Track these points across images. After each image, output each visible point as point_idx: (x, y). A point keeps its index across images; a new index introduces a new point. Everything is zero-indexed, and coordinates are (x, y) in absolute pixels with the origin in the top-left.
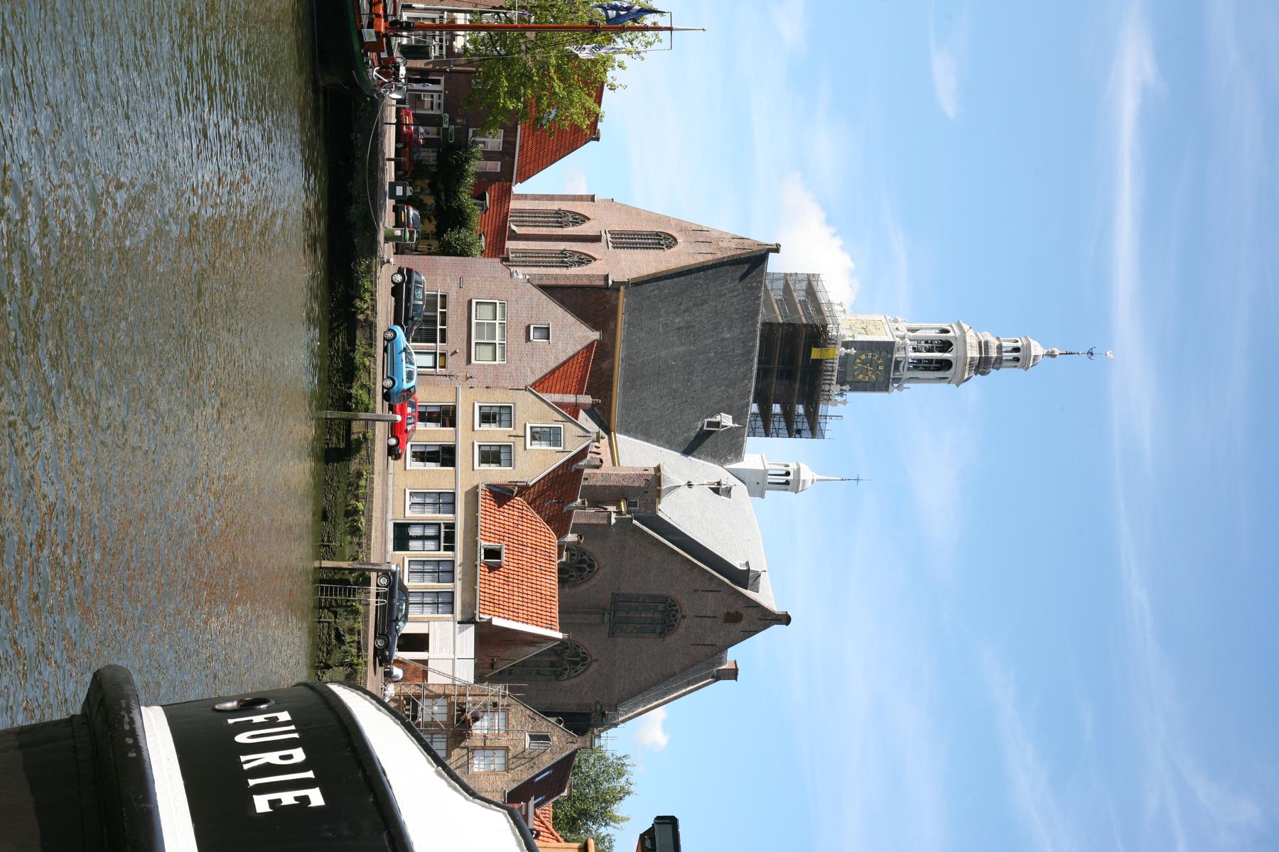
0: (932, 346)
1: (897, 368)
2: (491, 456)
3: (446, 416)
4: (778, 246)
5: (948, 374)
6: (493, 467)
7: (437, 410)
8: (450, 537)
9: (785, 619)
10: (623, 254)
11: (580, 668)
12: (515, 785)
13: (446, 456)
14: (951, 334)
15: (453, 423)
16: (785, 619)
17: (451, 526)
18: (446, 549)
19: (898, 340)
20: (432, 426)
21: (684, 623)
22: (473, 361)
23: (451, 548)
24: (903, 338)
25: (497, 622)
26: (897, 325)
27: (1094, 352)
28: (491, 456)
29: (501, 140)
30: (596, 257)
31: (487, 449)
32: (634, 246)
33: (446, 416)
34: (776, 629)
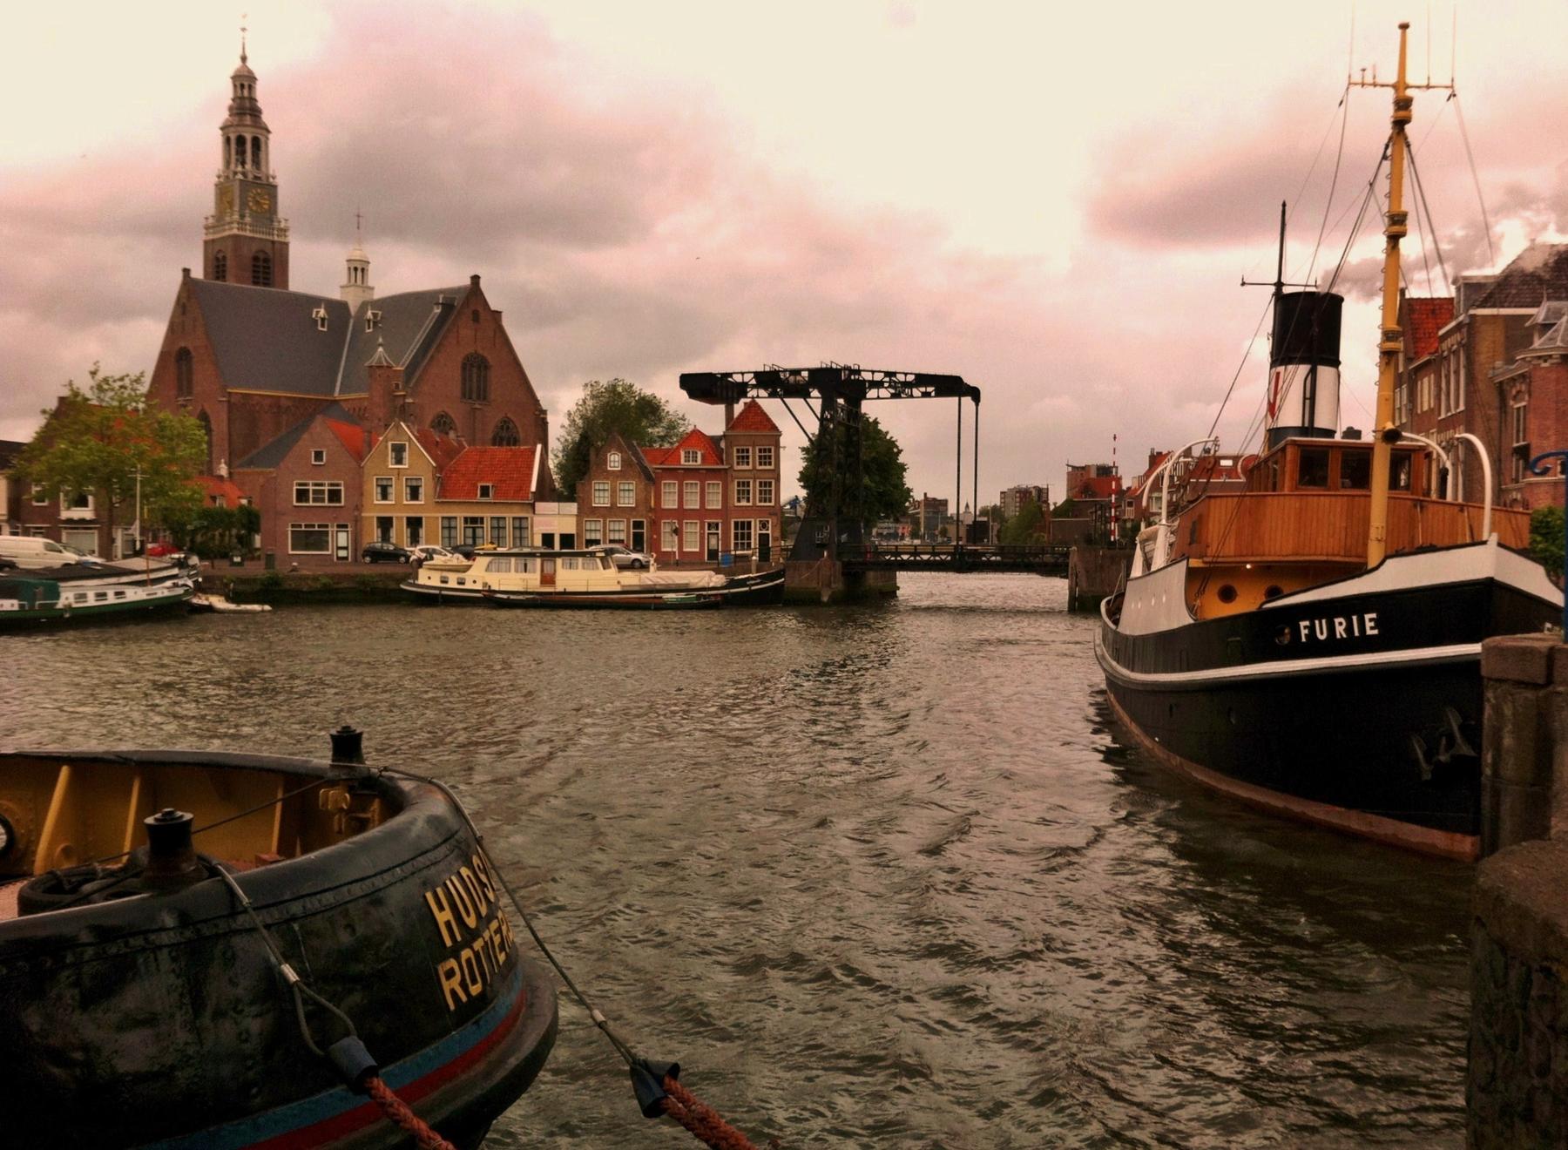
0: (241, 152)
1: (259, 178)
2: (414, 493)
3: (385, 524)
5: (262, 139)
6: (422, 491)
8: (474, 520)
9: (475, 279)
11: (511, 425)
13: (415, 524)
15: (390, 519)
16: (475, 279)
17: (466, 519)
18: (482, 523)
20: (393, 532)
21: (481, 352)
23: (482, 519)
25: (533, 488)
28: (414, 493)
32: (190, 381)
33: (385, 524)
34: (483, 285)
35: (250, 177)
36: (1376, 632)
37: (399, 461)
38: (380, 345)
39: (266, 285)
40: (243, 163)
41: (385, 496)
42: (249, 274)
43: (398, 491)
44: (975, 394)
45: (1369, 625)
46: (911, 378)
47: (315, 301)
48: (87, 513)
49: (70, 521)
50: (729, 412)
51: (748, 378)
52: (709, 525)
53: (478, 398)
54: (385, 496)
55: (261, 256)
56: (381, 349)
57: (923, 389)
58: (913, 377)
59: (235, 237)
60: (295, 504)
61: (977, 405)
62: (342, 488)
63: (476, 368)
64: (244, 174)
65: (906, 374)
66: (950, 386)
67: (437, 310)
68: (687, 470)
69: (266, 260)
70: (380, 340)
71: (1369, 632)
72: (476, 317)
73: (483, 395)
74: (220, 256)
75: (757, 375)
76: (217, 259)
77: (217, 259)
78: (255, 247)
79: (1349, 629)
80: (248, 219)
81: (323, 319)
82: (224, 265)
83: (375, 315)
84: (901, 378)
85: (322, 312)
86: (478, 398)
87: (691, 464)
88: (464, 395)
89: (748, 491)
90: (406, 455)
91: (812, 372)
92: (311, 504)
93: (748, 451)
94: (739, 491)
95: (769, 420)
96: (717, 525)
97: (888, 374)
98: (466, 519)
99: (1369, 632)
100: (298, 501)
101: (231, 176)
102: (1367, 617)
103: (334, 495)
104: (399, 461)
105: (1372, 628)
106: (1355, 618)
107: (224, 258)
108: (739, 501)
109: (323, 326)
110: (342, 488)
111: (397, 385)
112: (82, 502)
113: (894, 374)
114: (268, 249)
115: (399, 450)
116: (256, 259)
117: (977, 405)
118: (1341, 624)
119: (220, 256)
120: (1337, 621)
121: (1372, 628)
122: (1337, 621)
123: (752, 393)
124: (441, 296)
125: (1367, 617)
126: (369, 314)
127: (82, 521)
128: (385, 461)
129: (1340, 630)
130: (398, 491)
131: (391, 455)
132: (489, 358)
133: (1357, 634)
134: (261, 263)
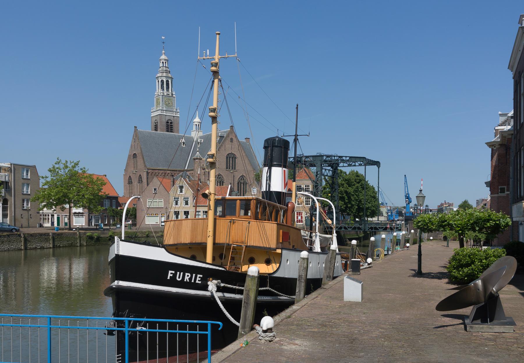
1: (169, 94)
2: (187, 203)
3: (177, 214)
6: (189, 202)
17: (203, 211)
22: (163, 207)
27: (163, 42)
28: (187, 203)
29: (107, 200)
31: (184, 203)
33: (177, 214)
35: (165, 94)
36: (200, 282)
37: (181, 192)
38: (198, 151)
39: (172, 132)
42: (165, 128)
43: (181, 202)
44: (377, 164)
45: (198, 279)
46: (348, 158)
49: (75, 213)
53: (232, 169)
54: (177, 204)
55: (170, 121)
57: (359, 163)
58: (349, 158)
65: (346, 157)
69: (171, 123)
70: (198, 150)
71: (197, 282)
72: (232, 140)
73: (234, 167)
76: (155, 123)
78: (167, 118)
79: (190, 279)
81: (184, 143)
82: (157, 125)
83: (201, 141)
86: (232, 169)
88: (227, 168)
90: (184, 189)
97: (340, 157)
98: (203, 211)
99: (197, 282)
102: (199, 276)
104: (181, 192)
105: (199, 280)
106: (194, 275)
107: (157, 122)
109: (183, 145)
113: (342, 157)
114: (172, 118)
115: (181, 187)
116: (167, 122)
118: (188, 276)
119: (156, 122)
120: (187, 274)
121: (199, 280)
122: (187, 274)
124: (220, 133)
125: (199, 276)
127: (79, 213)
129: (187, 278)
130: (181, 202)
131: (179, 190)
132: (236, 155)
133: (193, 281)
134: (169, 124)
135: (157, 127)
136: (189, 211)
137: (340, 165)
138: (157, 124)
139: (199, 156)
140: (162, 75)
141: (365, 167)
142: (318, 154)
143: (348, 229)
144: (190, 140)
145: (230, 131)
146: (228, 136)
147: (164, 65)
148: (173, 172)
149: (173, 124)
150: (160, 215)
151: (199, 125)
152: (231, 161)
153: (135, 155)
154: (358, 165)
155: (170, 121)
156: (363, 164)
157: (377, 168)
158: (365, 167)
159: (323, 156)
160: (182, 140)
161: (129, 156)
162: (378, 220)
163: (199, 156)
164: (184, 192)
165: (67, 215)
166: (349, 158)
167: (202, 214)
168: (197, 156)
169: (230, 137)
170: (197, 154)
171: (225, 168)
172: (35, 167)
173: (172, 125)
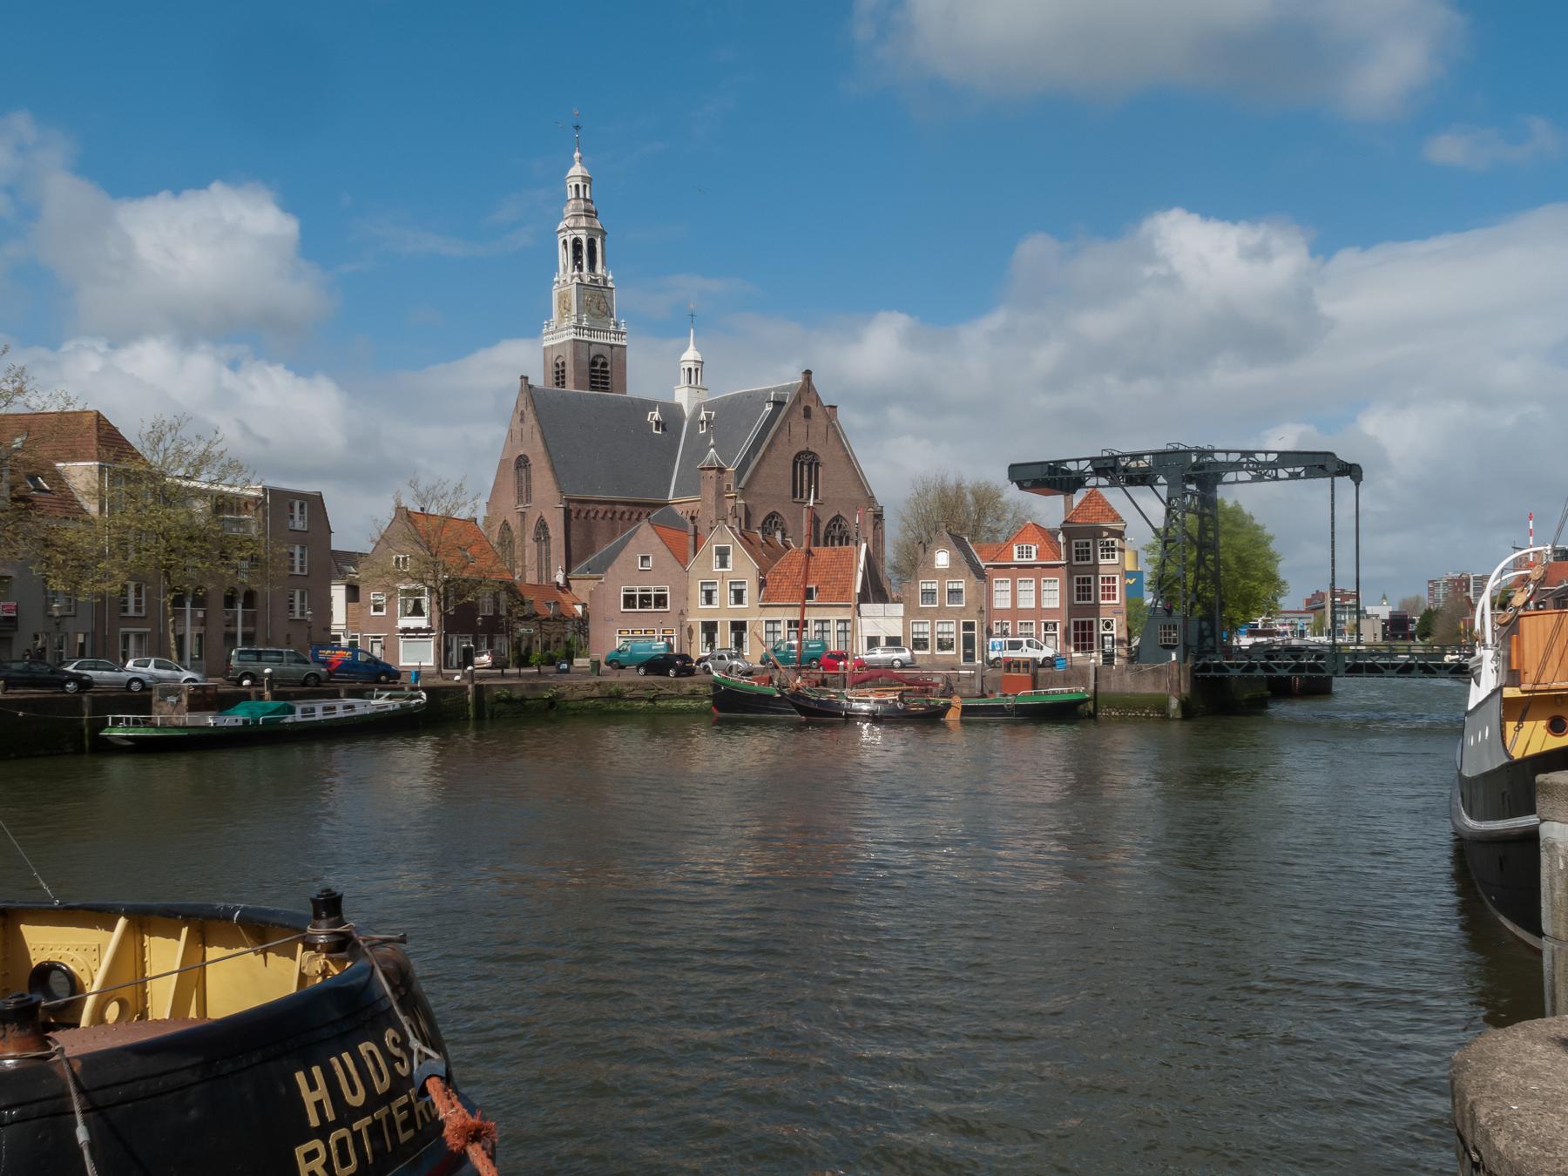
1: (596, 281)
2: (739, 597)
3: (710, 628)
4: (522, 377)
6: (745, 593)
7: (704, 635)
9: (808, 373)
10: (536, 495)
12: (973, 575)
14: (567, 238)
15: (715, 624)
16: (808, 373)
19: (574, 281)
20: (718, 637)
22: (668, 609)
24: (573, 277)
25: (858, 590)
26: (561, 282)
28: (739, 597)
30: (538, 516)
32: (529, 488)
33: (710, 628)
34: (815, 380)
35: (587, 280)
37: (723, 564)
38: (713, 446)
40: (580, 268)
41: (709, 600)
43: (723, 595)
46: (1272, 457)
47: (649, 405)
48: (422, 622)
49: (406, 630)
50: (1068, 504)
51: (1083, 465)
52: (1046, 625)
54: (709, 600)
56: (712, 450)
57: (1291, 470)
58: (1275, 456)
59: (575, 340)
60: (622, 610)
61: (1357, 484)
62: (668, 593)
63: (806, 463)
64: (580, 277)
66: (1321, 465)
67: (769, 408)
68: (1020, 567)
70: (712, 441)
72: (807, 413)
74: (559, 361)
75: (1093, 460)
76: (557, 365)
77: (557, 365)
78: (593, 352)
80: (584, 324)
82: (563, 371)
84: (1261, 457)
85: (657, 415)
87: (1025, 561)
88: (795, 495)
89: (1089, 588)
90: (730, 558)
91: (1156, 454)
92: (638, 610)
93: (1088, 544)
94: (1078, 588)
95: (1111, 510)
96: (1055, 625)
97: (1245, 453)
98: (790, 623)
100: (625, 607)
101: (569, 281)
103: (661, 600)
104: (723, 564)
107: (563, 364)
108: (1078, 599)
109: (657, 429)
110: (668, 593)
111: (729, 487)
112: (417, 611)
113: (1252, 453)
114: (606, 352)
115: (723, 553)
116: (594, 363)
117: (1357, 484)
119: (559, 361)
123: (1091, 482)
124: (773, 393)
126: (703, 416)
128: (710, 566)
130: (723, 595)
131: (716, 559)
134: (598, 368)
135: (563, 377)
136: (715, 623)
137: (1224, 479)
138: (561, 368)
139: (717, 461)
140: (578, 225)
141: (1333, 482)
142: (1170, 447)
143: (1275, 671)
144: (672, 415)
145: (804, 384)
146: (798, 399)
147: (581, 195)
148: (636, 508)
149: (608, 368)
150: (659, 632)
151: (697, 370)
152: (806, 474)
153: (522, 463)
154: (1287, 476)
155: (600, 361)
156: (1303, 474)
157: (1353, 483)
158: (1333, 482)
159: (1190, 451)
160: (653, 415)
161: (503, 462)
162: (1359, 643)
163: (717, 461)
164: (730, 564)
165: (379, 637)
166: (1275, 456)
167: (787, 629)
168: (712, 460)
169: (804, 404)
170: (709, 456)
171: (791, 494)
172: (321, 496)
173: (607, 372)
